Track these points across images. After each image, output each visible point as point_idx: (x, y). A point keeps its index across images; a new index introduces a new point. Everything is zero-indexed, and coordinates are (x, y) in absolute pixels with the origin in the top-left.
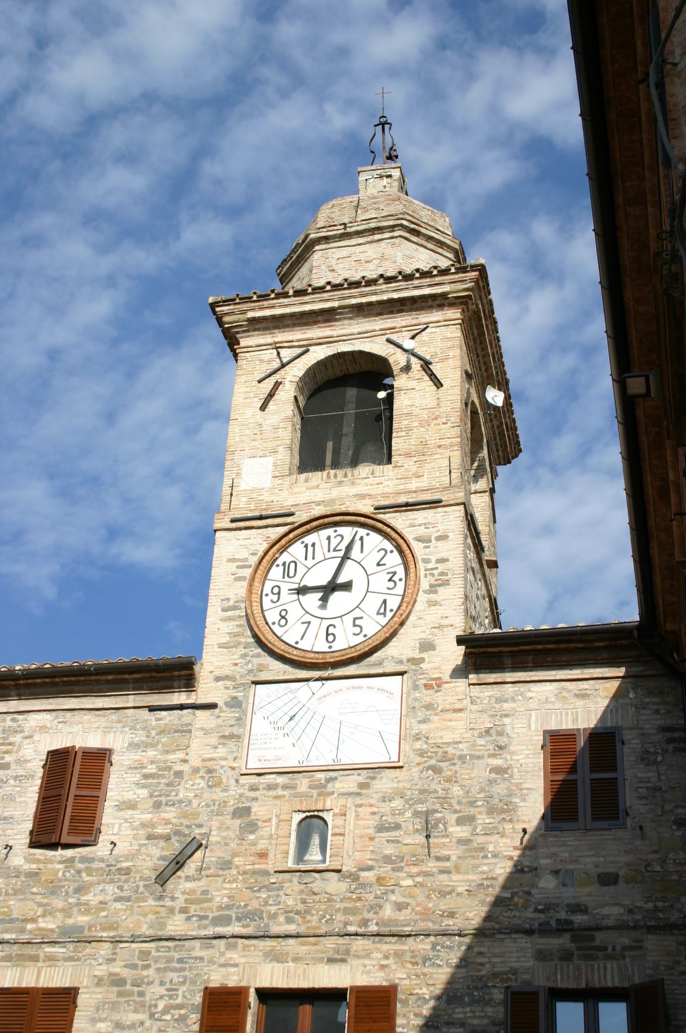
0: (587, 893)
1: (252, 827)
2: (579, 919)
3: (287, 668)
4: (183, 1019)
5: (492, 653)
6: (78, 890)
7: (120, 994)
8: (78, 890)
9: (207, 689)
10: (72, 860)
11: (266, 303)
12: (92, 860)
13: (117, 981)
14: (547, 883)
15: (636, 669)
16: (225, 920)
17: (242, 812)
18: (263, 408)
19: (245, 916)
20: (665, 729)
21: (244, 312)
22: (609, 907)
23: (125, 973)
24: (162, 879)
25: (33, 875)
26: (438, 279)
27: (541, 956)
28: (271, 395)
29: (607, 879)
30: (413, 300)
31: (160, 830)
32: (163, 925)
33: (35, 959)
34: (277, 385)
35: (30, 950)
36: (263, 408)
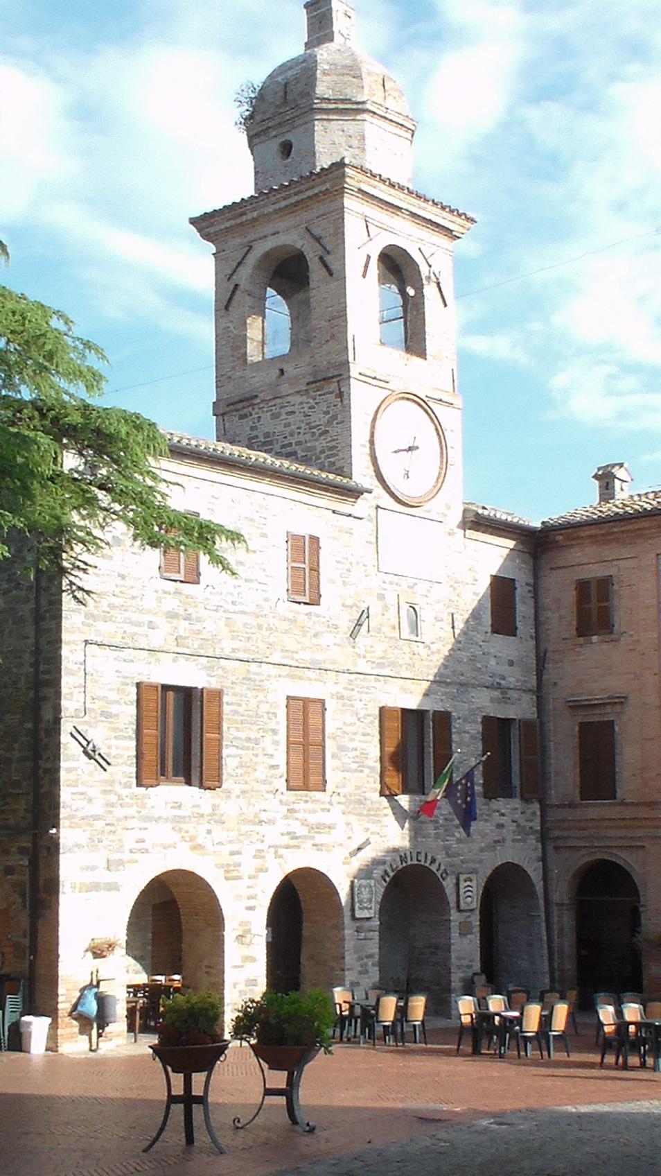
0: (504, 669)
1: (386, 608)
2: (503, 682)
3: (392, 500)
4: (372, 722)
5: (478, 523)
6: (316, 635)
7: (344, 705)
8: (316, 635)
9: (362, 506)
10: (308, 614)
11: (372, 182)
12: (318, 616)
13: (342, 698)
14: (493, 662)
15: (521, 547)
16: (380, 665)
17: (381, 597)
18: (364, 276)
19: (392, 664)
20: (527, 584)
21: (359, 181)
22: (513, 677)
23: (345, 693)
24: (353, 635)
25: (294, 621)
26: (454, 219)
27: (492, 700)
28: (366, 266)
29: (511, 663)
30: (437, 225)
31: (349, 602)
32: (355, 665)
33: (301, 678)
34: (369, 257)
35: (298, 672)
36: (364, 276)
